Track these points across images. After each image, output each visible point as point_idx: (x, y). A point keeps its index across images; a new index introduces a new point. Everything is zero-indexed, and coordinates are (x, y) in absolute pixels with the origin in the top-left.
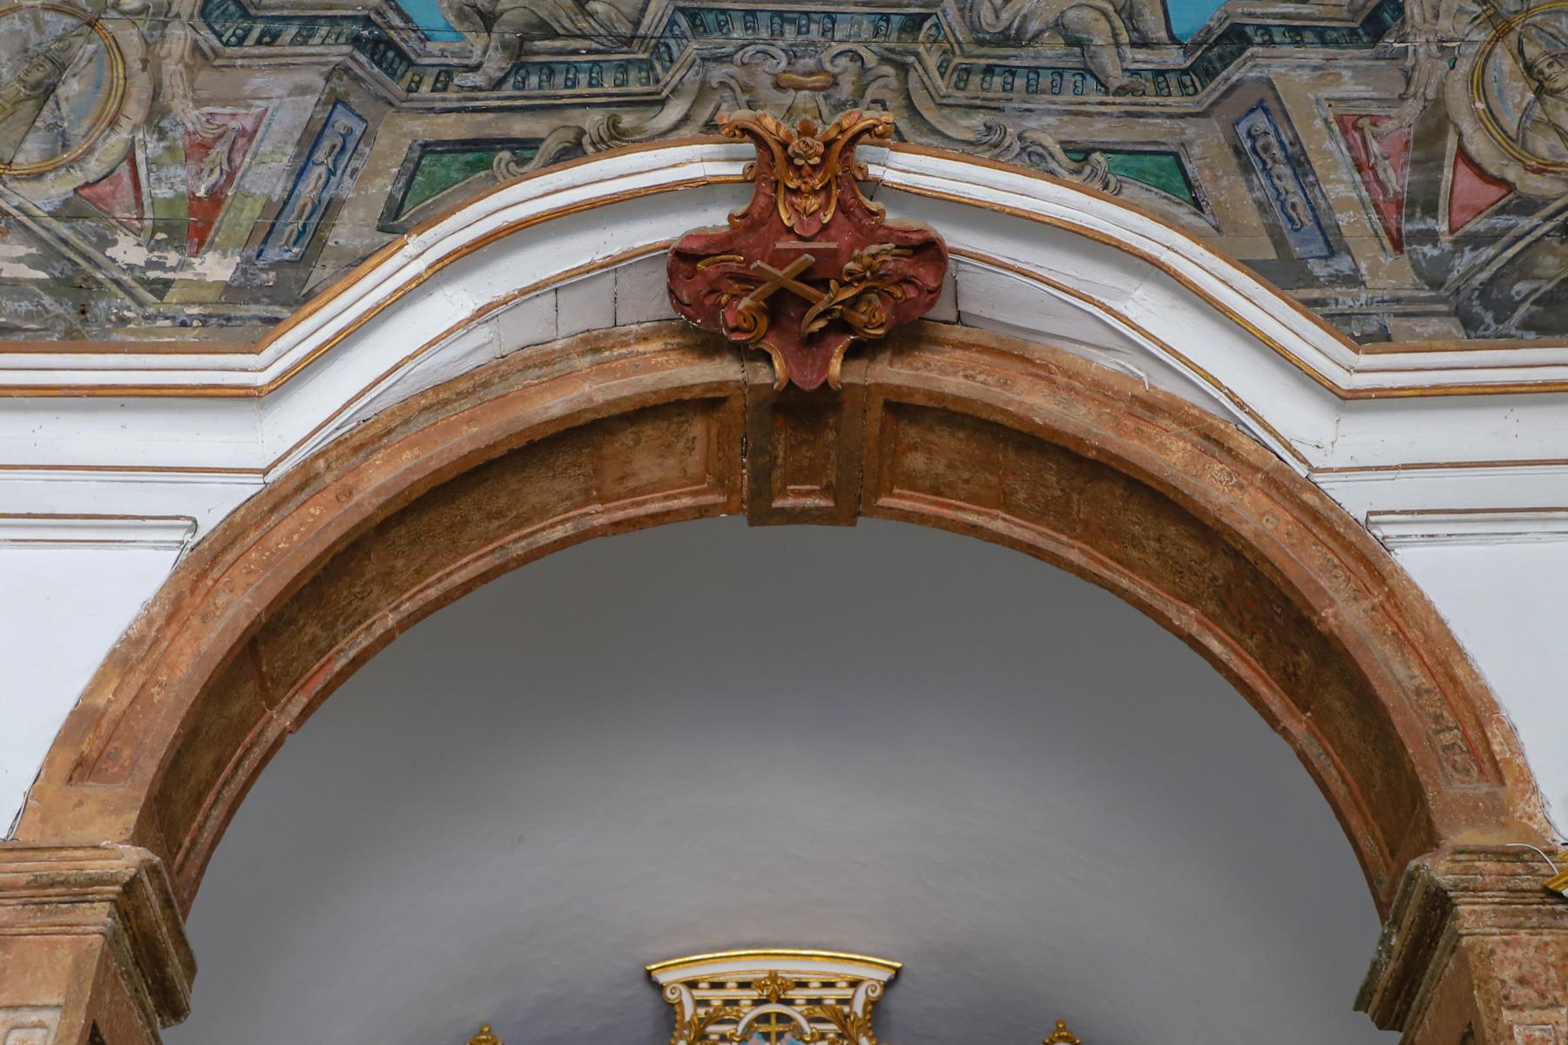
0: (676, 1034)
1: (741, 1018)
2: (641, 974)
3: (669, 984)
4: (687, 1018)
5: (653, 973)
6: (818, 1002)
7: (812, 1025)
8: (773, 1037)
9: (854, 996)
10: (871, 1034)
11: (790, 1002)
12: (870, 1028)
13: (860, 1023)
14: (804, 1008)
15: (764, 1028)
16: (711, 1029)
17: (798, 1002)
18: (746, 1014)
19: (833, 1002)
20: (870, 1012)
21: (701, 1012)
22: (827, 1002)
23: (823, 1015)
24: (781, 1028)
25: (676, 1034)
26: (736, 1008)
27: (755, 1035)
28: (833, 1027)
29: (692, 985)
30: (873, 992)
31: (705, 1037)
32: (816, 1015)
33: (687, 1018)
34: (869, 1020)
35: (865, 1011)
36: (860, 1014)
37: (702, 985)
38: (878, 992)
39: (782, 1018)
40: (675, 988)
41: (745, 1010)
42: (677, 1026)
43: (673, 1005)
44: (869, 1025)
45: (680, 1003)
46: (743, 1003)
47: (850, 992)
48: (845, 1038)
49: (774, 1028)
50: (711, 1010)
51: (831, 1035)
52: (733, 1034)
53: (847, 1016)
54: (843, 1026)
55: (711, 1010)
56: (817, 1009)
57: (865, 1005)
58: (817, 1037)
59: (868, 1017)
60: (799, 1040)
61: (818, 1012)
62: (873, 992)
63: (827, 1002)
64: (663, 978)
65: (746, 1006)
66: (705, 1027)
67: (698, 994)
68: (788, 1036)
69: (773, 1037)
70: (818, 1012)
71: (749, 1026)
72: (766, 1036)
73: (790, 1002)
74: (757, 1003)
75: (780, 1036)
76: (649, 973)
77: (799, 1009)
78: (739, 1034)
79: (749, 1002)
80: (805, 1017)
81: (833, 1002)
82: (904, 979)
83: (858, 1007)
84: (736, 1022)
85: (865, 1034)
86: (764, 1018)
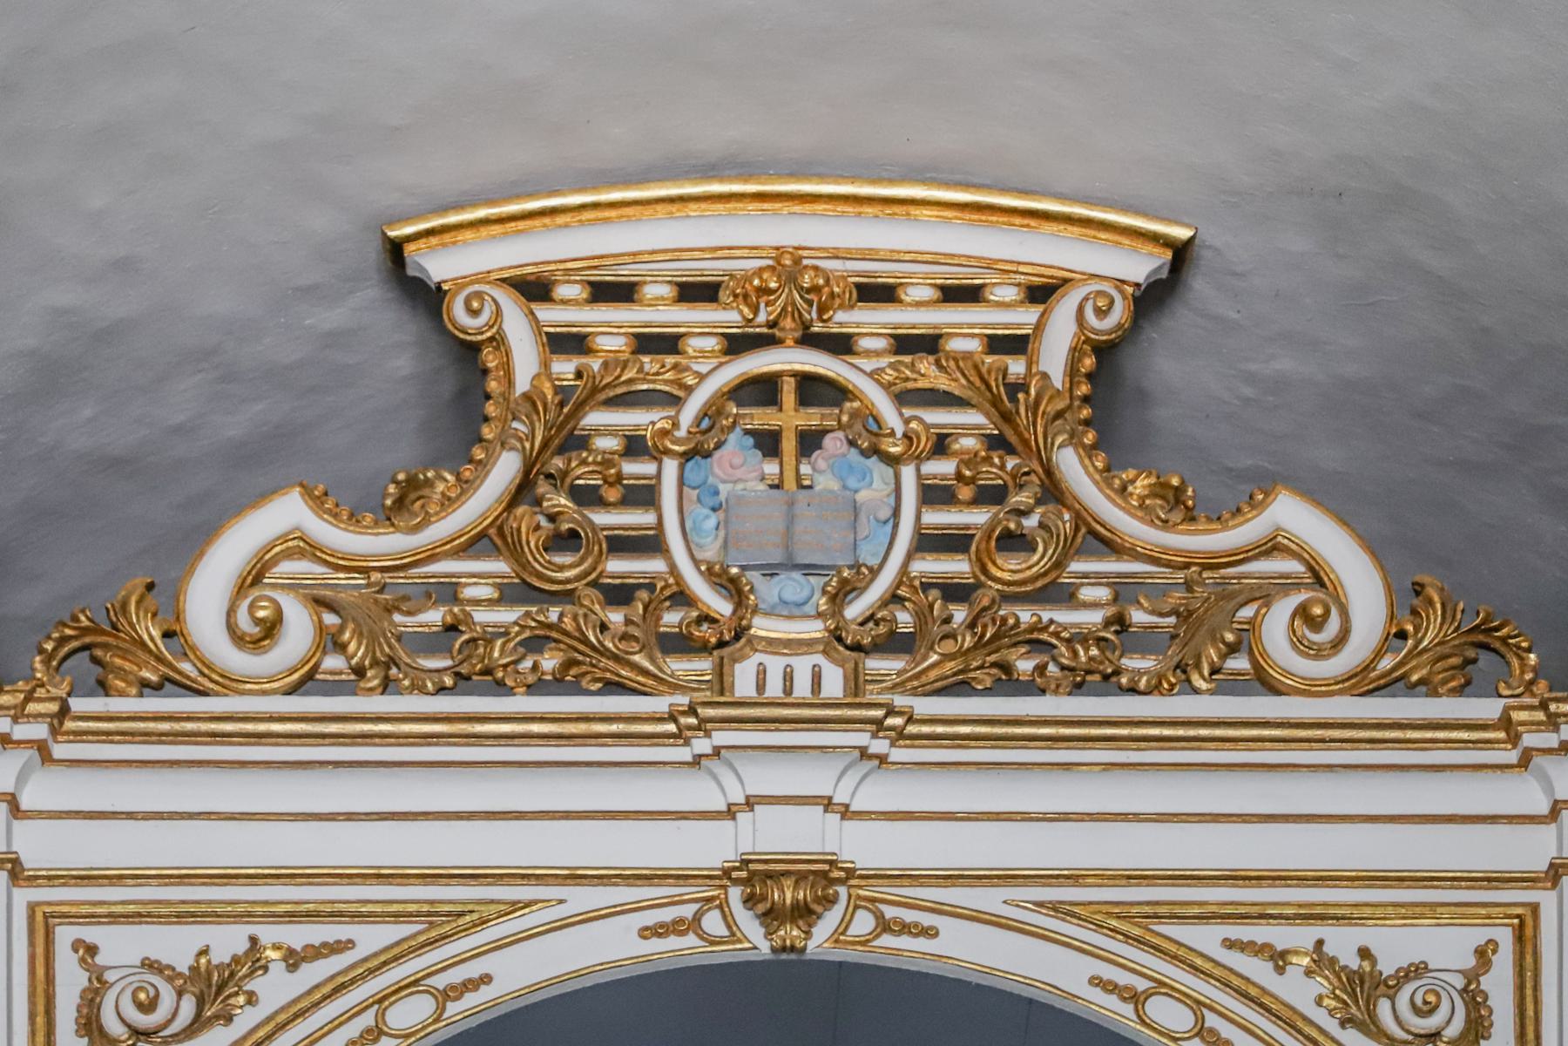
0: (488, 432)
1: (690, 390)
2: (373, 254)
3: (461, 283)
4: (522, 384)
5: (409, 249)
6: (927, 344)
7: (907, 412)
8: (789, 445)
9: (1039, 327)
10: (1089, 438)
11: (841, 345)
12: (1087, 423)
13: (1060, 405)
14: (884, 361)
15: (762, 418)
16: (594, 418)
17: (865, 343)
18: (702, 377)
19: (974, 345)
20: (1090, 376)
21: (565, 367)
22: (955, 345)
23: (943, 383)
24: (812, 418)
25: (488, 432)
26: (670, 360)
27: (734, 438)
28: (974, 418)
29: (534, 289)
30: (1101, 313)
31: (576, 442)
32: (921, 384)
33: (522, 384)
34: (1086, 399)
35: (1072, 371)
36: (1058, 379)
37: (563, 291)
38: (1119, 313)
39: (813, 389)
40: (479, 295)
41: (703, 368)
42: (491, 409)
43: (475, 348)
44: (1086, 413)
45: (498, 341)
46: (693, 345)
47: (1027, 317)
48: (1011, 450)
49: (790, 418)
50: (596, 364)
51: (969, 443)
52: (665, 433)
53: (1015, 388)
54: (1007, 418)
55: (596, 364)
56: (926, 365)
57: (1075, 354)
58: (924, 444)
59: (1084, 389)
60: (865, 454)
61: (927, 372)
62: (1101, 313)
63: (955, 345)
64: (437, 265)
65: (703, 354)
66: (580, 408)
67: (548, 314)
68: (834, 443)
69: (789, 445)
70: (927, 372)
71: (712, 412)
72: (768, 443)
73: (841, 345)
74: (736, 345)
75: (810, 442)
76: (396, 250)
77: (868, 365)
78: (681, 433)
79: (711, 343)
80: (887, 387)
81: (974, 345)
82: (1199, 284)
83: (1054, 356)
84: (675, 401)
85: (1074, 439)
86: (763, 389)
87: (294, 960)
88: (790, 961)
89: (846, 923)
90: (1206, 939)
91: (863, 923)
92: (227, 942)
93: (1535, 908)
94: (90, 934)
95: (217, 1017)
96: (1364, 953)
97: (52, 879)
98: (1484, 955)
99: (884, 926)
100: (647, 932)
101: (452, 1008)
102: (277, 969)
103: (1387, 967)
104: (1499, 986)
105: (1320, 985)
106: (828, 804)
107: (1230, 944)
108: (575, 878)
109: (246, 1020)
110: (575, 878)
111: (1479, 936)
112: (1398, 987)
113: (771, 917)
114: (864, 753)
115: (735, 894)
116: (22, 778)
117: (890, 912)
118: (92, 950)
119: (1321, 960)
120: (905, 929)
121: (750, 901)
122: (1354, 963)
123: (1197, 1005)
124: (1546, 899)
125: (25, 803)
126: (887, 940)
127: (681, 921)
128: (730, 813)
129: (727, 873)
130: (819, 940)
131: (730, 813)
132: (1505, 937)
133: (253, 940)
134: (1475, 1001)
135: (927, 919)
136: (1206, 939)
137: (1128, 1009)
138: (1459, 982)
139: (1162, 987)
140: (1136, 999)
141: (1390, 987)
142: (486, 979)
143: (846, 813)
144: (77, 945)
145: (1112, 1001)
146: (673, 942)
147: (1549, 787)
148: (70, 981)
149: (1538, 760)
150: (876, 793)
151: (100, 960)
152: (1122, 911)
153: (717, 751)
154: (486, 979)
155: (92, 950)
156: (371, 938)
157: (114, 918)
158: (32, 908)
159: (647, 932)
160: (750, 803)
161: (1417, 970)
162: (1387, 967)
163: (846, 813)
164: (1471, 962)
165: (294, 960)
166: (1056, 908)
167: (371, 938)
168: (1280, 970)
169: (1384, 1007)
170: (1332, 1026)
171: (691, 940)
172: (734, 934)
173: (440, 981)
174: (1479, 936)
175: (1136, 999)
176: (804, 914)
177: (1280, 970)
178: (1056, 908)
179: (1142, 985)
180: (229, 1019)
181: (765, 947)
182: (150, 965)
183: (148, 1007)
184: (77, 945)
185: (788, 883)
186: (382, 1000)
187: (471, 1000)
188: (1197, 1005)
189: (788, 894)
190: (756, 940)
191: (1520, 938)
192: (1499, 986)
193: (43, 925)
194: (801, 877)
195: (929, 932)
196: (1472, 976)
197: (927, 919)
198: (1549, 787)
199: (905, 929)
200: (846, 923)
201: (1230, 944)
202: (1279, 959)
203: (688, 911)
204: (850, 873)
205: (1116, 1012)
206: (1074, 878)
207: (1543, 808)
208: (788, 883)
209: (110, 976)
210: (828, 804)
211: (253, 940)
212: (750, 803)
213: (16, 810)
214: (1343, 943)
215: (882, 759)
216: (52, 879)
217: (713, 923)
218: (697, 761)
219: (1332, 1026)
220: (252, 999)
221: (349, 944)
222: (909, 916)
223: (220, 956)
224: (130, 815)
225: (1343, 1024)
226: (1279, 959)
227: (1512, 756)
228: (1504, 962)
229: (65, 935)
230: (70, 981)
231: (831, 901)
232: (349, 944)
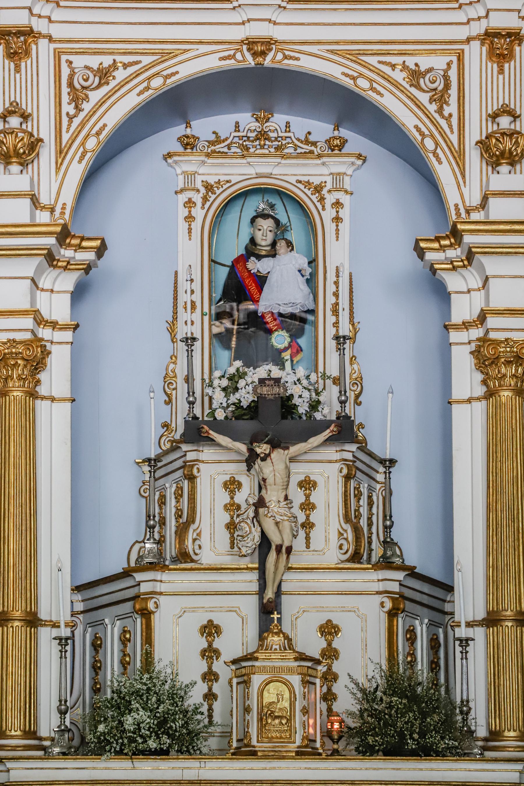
87: (125, 66)
88: (259, 69)
89: (275, 56)
90: (373, 60)
91: (280, 56)
92: (107, 61)
93: (463, 50)
94: (71, 58)
95: (105, 83)
96: (416, 65)
97: (60, 41)
98: (449, 64)
99: (285, 57)
100: (222, 59)
101: (169, 81)
102: (121, 68)
103: (423, 69)
104: (453, 74)
105: (404, 74)
106: (270, 21)
107: (380, 62)
108: (201, 43)
109: (113, 84)
110: (201, 43)
111: (447, 59)
112: (425, 75)
113: (255, 55)
114: (280, 6)
115: (245, 47)
116: (52, 12)
117: (287, 53)
118: (71, 63)
119: (405, 68)
120: (291, 58)
121: (249, 50)
122: (413, 67)
123: (371, 81)
124: (466, 47)
125: (53, 19)
126: (286, 61)
127: (230, 56)
128: (243, 23)
129: (242, 41)
130: (268, 62)
131: (243, 23)
132: (455, 59)
133: (114, 60)
134: (446, 78)
135: (297, 55)
136: (373, 60)
137: (352, 82)
138: (442, 73)
139: (361, 75)
140: (354, 79)
141: (423, 75)
142: (177, 73)
143: (275, 23)
144: (67, 61)
145: (347, 80)
146: (228, 62)
147: (467, 15)
148: (65, 72)
149: (464, 7)
150: (283, 17)
151: (73, 65)
152: (350, 52)
153: (240, 6)
154: (177, 73)
155: (71, 63)
156: (146, 60)
157: (77, 53)
158: (55, 49)
159: (222, 59)
160: (249, 21)
161: (430, 70)
162: (423, 69)
163: (275, 23)
164: (445, 67)
165: (125, 66)
166: (332, 52)
167: (146, 60)
168: (393, 70)
169: (422, 81)
170: (407, 86)
171: (233, 61)
172: (244, 61)
173: (165, 73)
174: (447, 59)
175: (354, 79)
176: (263, 54)
177: (393, 70)
178: (332, 52)
179: (356, 74)
180: (108, 84)
181: (253, 64)
182: (87, 67)
183: (86, 80)
184: (67, 61)
185: (259, 45)
186: (149, 79)
187: (173, 79)
188: (371, 81)
189: (259, 48)
190: (251, 61)
191: (459, 60)
192: (453, 74)
193: (58, 54)
194: (262, 43)
195: (297, 59)
196: (446, 71)
197: (297, 55)
198: (467, 15)
199: (291, 58)
200: (275, 56)
201: (380, 62)
202: (393, 66)
203: (232, 52)
204: (276, 41)
205: (348, 82)
206: (337, 43)
207: (465, 21)
208: (259, 45)
209: (76, 71)
210: (270, 21)
211: (114, 60)
212: (249, 21)
213: (50, 21)
214: (410, 61)
215: (285, 8)
216: (60, 41)
217: (239, 56)
218: (234, 8)
219: (407, 86)
220: (114, 78)
221: (140, 62)
222: (292, 54)
223: (105, 65)
224: (81, 23)
225: (411, 86)
226: (393, 66)
227: (456, 5)
228: (454, 66)
229: (64, 58)
230: (65, 72)
231: (270, 50)
232: (140, 62)
